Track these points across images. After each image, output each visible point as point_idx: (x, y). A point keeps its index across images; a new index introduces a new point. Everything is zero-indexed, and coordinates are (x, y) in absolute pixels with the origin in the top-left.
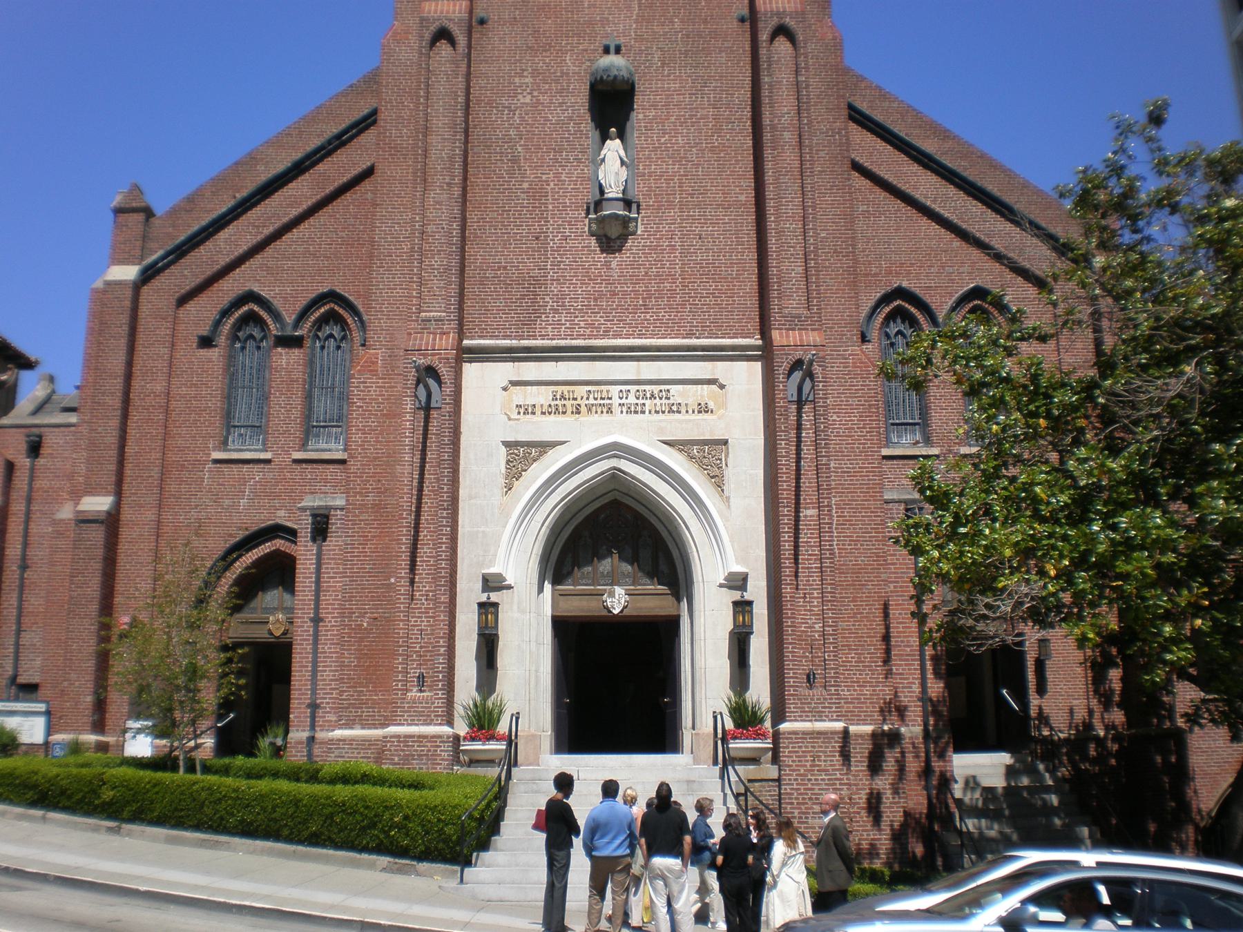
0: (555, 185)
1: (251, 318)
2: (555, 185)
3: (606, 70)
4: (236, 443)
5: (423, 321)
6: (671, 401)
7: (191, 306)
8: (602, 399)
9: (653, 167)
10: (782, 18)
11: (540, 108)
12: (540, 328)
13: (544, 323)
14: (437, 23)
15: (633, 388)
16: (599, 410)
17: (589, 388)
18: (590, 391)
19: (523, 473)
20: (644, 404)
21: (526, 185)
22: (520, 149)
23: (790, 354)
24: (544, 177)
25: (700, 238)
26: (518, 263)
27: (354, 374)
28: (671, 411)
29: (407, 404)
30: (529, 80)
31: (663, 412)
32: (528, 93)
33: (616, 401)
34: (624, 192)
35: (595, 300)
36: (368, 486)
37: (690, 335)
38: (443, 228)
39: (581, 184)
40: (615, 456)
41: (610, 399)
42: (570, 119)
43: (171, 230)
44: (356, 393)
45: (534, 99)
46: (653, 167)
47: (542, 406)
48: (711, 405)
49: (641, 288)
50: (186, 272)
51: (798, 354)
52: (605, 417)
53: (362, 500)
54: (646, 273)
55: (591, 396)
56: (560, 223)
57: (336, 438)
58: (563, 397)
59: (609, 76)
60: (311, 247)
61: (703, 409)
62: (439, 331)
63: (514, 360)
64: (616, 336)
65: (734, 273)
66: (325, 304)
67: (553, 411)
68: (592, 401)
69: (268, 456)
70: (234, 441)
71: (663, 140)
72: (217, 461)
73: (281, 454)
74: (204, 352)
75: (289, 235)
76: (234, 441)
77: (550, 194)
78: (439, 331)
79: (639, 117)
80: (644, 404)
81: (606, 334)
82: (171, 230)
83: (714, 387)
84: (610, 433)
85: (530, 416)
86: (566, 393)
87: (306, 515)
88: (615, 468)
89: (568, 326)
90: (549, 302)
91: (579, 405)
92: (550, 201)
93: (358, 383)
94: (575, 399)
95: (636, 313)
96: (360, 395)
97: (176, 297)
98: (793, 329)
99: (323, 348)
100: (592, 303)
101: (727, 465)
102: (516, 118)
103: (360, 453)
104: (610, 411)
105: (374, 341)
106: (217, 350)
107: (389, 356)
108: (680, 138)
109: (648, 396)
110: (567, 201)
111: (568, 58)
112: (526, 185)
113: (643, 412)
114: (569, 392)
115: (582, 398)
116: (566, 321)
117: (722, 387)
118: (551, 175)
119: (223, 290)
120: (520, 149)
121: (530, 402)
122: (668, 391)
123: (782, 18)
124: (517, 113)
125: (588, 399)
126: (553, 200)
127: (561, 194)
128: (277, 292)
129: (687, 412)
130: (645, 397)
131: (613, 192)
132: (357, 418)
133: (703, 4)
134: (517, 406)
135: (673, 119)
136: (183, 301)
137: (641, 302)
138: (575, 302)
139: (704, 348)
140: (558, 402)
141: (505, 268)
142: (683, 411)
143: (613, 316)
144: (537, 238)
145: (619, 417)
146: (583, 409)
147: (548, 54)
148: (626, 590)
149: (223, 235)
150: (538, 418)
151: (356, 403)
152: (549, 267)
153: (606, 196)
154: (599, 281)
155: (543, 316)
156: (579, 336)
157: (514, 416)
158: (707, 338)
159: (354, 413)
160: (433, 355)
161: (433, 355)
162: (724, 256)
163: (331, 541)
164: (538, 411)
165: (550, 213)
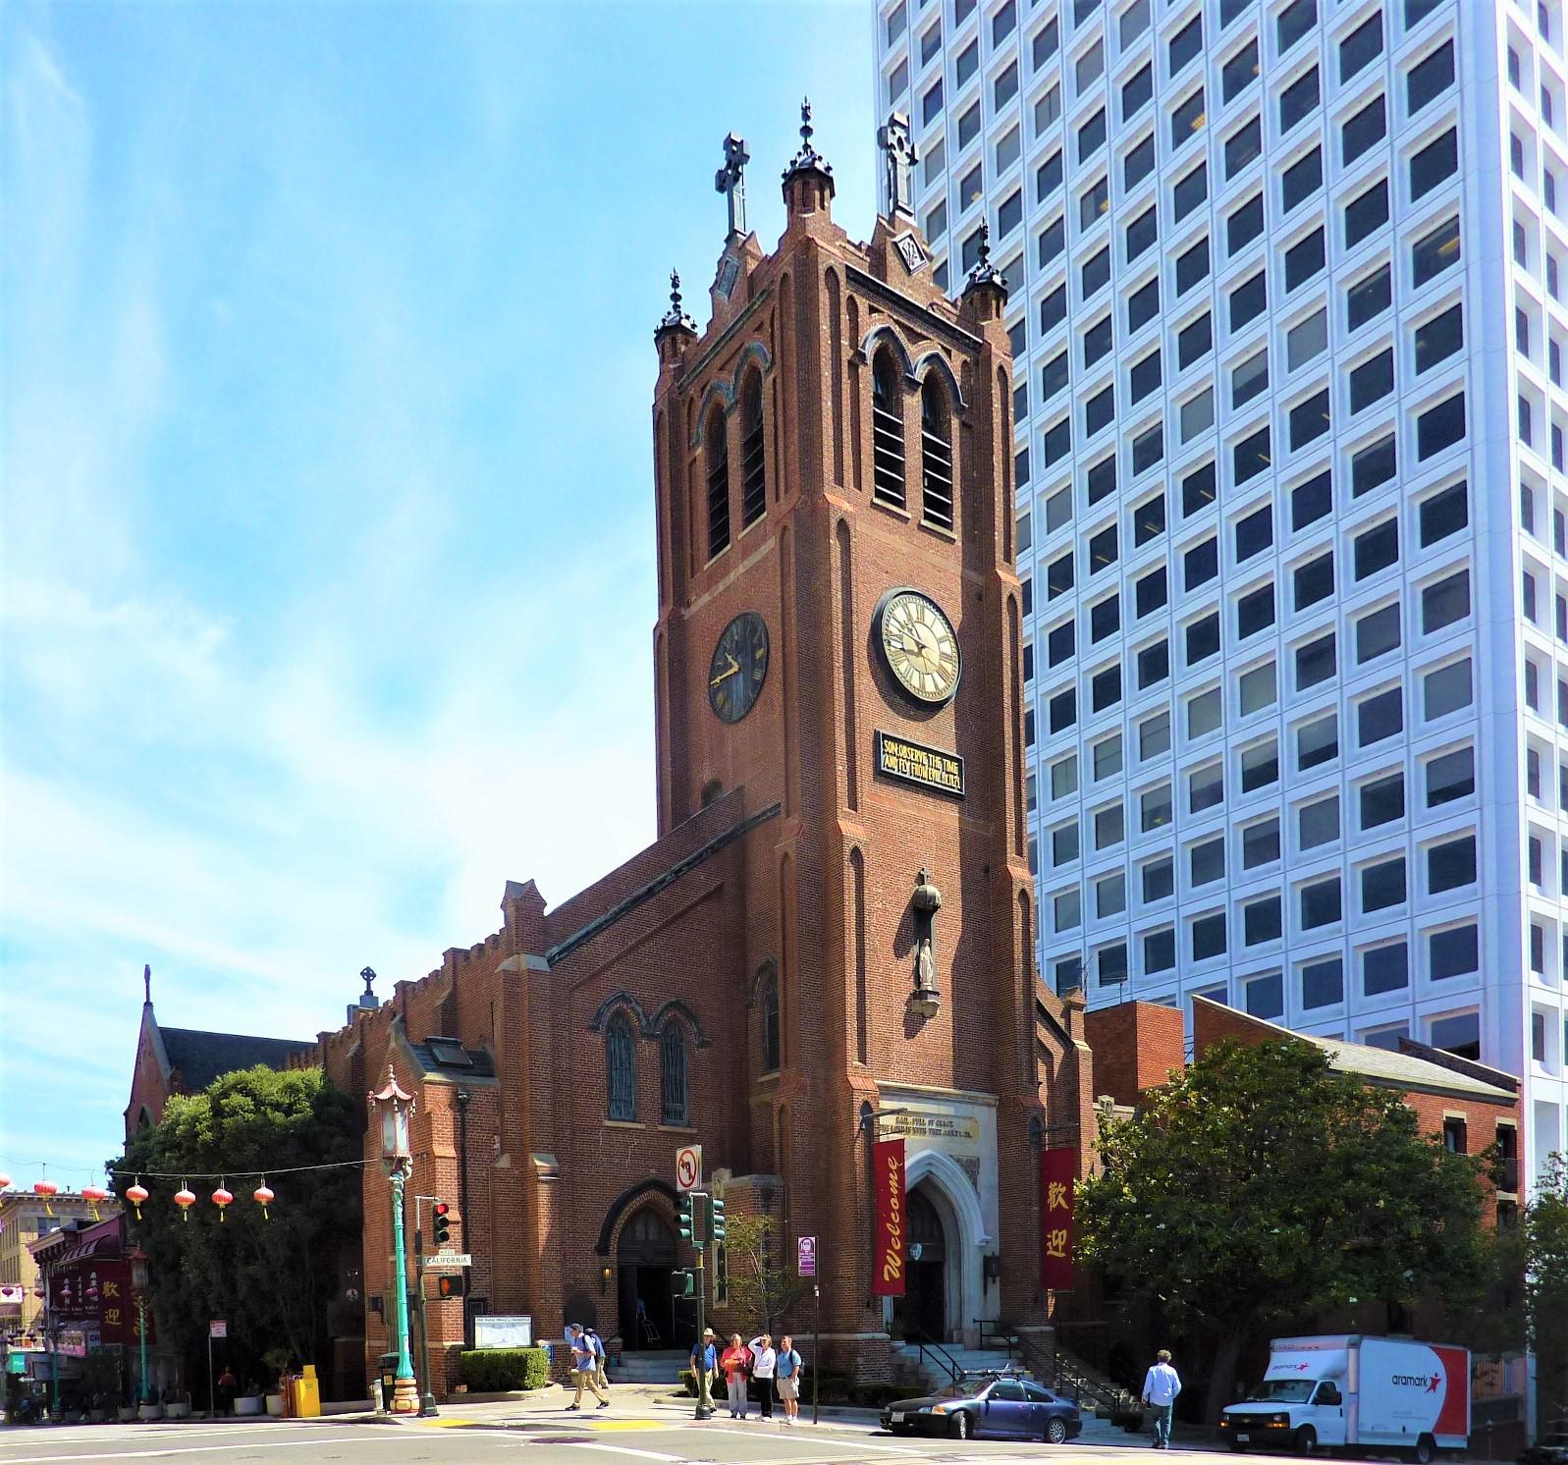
33: (927, 1127)
40: (930, 1164)
64: (928, 1084)
81: (922, 1083)
145: (928, 1138)
156: (910, 1082)
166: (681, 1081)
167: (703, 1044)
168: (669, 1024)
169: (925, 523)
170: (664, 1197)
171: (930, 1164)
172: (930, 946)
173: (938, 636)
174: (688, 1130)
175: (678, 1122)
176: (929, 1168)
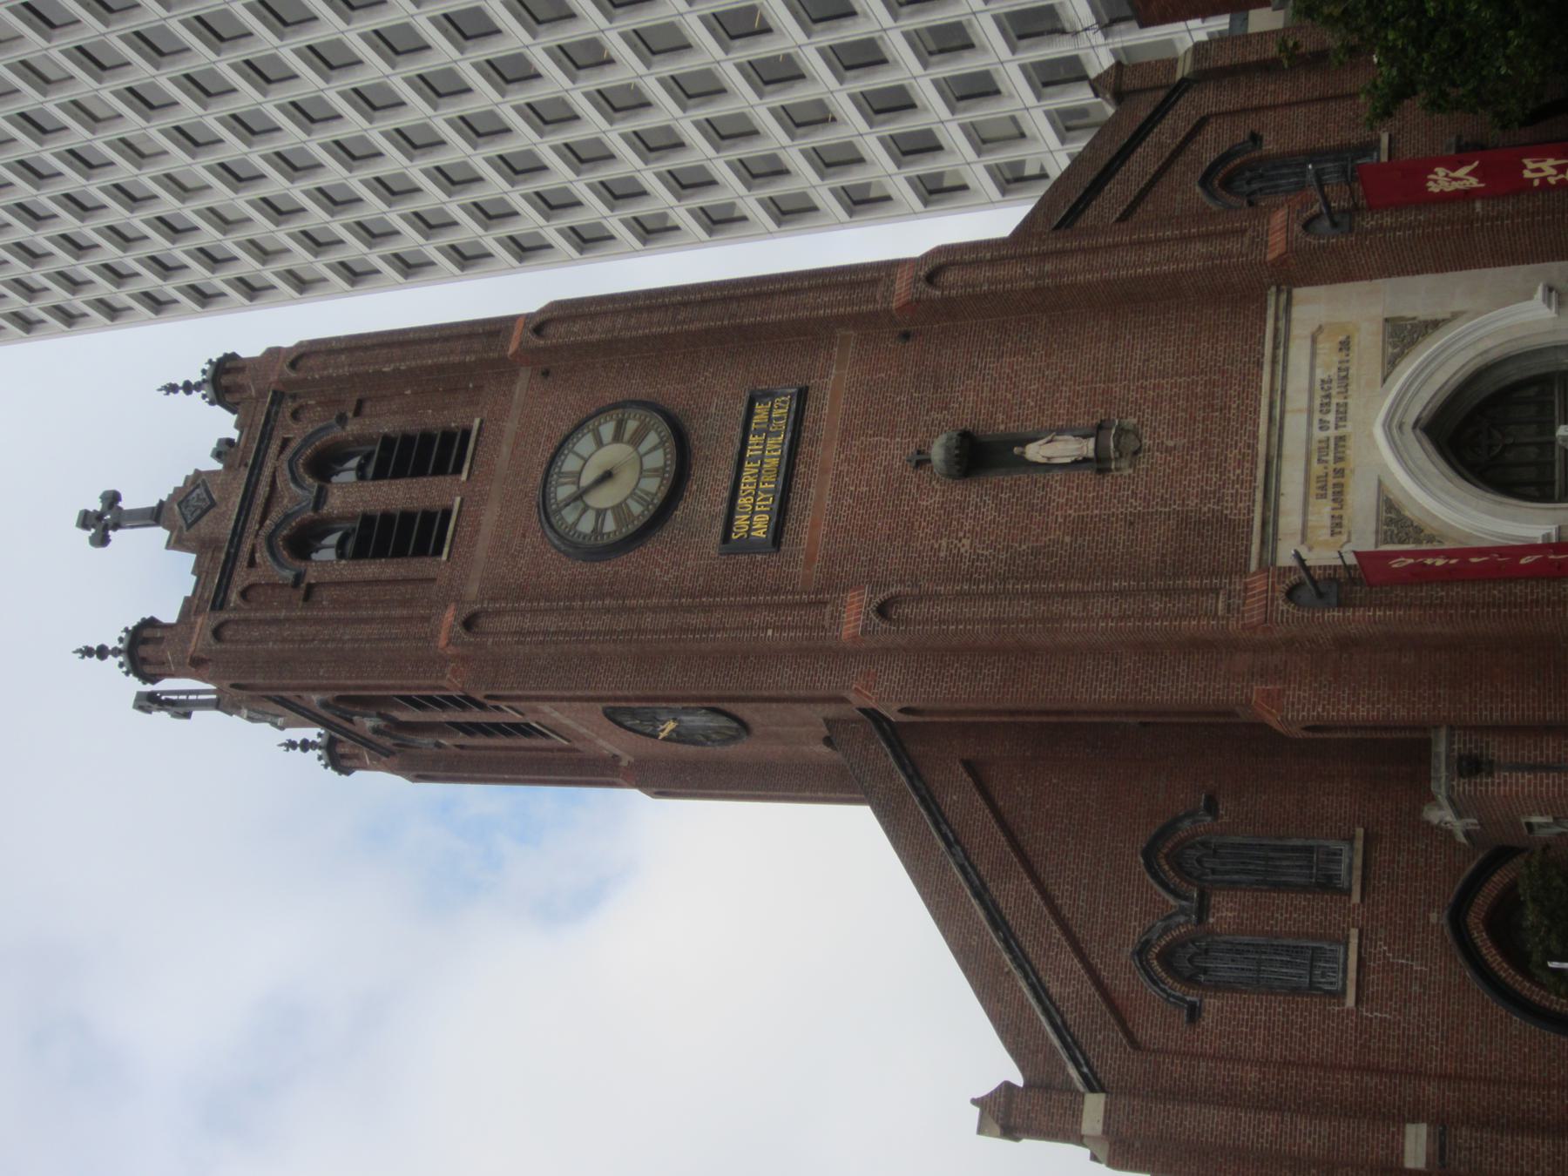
0: (1071, 508)
1: (1167, 958)
2: (1071, 508)
3: (947, 449)
4: (1334, 980)
5: (1229, 612)
6: (1335, 377)
7: (1141, 1035)
8: (1328, 447)
9: (1062, 411)
10: (920, 279)
11: (978, 529)
12: (1240, 514)
13: (1234, 511)
14: (872, 615)
15: (1317, 416)
16: (1340, 449)
17: (1314, 460)
18: (1319, 460)
19: (1415, 524)
20: (1337, 404)
21: (1067, 539)
22: (1024, 547)
23: (1297, 236)
24: (1060, 520)
25: (1148, 360)
26: (1159, 542)
27: (1282, 717)
28: (1346, 377)
29: (1334, 616)
30: (944, 542)
31: (1347, 385)
32: (960, 541)
33: (1332, 433)
34: (1085, 437)
35: (1209, 460)
36: (1426, 695)
37: (1260, 365)
38: (1117, 600)
39: (1073, 482)
40: (1400, 426)
41: (1328, 439)
42: (995, 497)
43: (1040, 1056)
44: (1305, 713)
45: (967, 535)
46: (1062, 411)
47: (1333, 509)
48: (1342, 338)
49: (1200, 415)
50: (1100, 1037)
51: (1297, 228)
52: (1350, 443)
53: (1444, 700)
54: (1183, 410)
55: (1324, 458)
56: (1116, 501)
57: (1335, 854)
58: (1324, 488)
59: (956, 448)
60: (1083, 881)
61: (1345, 345)
62: (1243, 594)
63: (1275, 539)
64: (1255, 436)
65: (1191, 325)
66: (1160, 866)
67: (1339, 497)
68: (1331, 457)
69: (1354, 932)
70: (1331, 983)
71: (1032, 404)
72: (1358, 1001)
73: (1353, 918)
74: (1208, 1020)
75: (1065, 911)
76: (1331, 983)
77: (1081, 513)
78: (1243, 594)
79: (1002, 426)
80: (1337, 404)
82: (1040, 1056)
83: (1321, 338)
84: (1371, 436)
85: (1345, 522)
86: (1319, 484)
87: (1458, 785)
88: (1414, 427)
89: (1239, 486)
90: (1209, 508)
91: (1335, 470)
92: (1089, 512)
93: (1293, 711)
94: (1327, 475)
95: (1229, 418)
96: (1309, 710)
97: (1132, 1051)
98: (1267, 242)
99: (1214, 871)
100: (1214, 462)
101: (1414, 318)
102: (985, 553)
103: (1384, 706)
104: (1341, 439)
105: (1242, 695)
106: (1207, 1000)
107: (1262, 676)
108: (1033, 387)
109: (1327, 400)
110: (1091, 495)
111: (925, 503)
112: (1067, 539)
113: (1346, 404)
114: (1318, 482)
115: (1326, 468)
116: (1233, 488)
117: (1320, 328)
118: (1059, 513)
119: (1128, 992)
120: (1024, 547)
121: (1327, 522)
122: (1323, 381)
123: (920, 279)
124: (980, 552)
125: (1326, 462)
126: (1088, 509)
127: (1082, 502)
128: (1137, 924)
129: (1348, 361)
130: (1328, 404)
131: (1088, 447)
132: (1339, 710)
133: (883, 375)
134: (1333, 534)
135: (1009, 396)
136: (1134, 1043)
137: (1217, 414)
138: (1211, 479)
139: (1275, 347)
140: (1330, 492)
141: (1163, 555)
142: (1344, 366)
143: (1232, 440)
144: (1131, 523)
145: (1349, 428)
146: (1340, 465)
147: (917, 524)
148: (1560, 424)
149: (1055, 989)
150: (1347, 513)
151: (1318, 712)
152: (1167, 510)
153: (1091, 454)
154: (1189, 458)
155: (1225, 512)
156: (1253, 474)
157: (1344, 538)
158: (1263, 347)
159: (1331, 713)
160: (1273, 590)
161: (1273, 590)
162: (1171, 336)
163: (1493, 755)
164: (1337, 513)
165: (1103, 512)
166: (1275, 848)
167: (1211, 807)
168: (1179, 868)
169: (464, 476)
170: (1479, 900)
171: (1400, 426)
172: (1025, 441)
173: (593, 446)
174: (1359, 845)
175: (1345, 860)
176: (1408, 428)
